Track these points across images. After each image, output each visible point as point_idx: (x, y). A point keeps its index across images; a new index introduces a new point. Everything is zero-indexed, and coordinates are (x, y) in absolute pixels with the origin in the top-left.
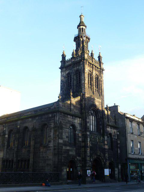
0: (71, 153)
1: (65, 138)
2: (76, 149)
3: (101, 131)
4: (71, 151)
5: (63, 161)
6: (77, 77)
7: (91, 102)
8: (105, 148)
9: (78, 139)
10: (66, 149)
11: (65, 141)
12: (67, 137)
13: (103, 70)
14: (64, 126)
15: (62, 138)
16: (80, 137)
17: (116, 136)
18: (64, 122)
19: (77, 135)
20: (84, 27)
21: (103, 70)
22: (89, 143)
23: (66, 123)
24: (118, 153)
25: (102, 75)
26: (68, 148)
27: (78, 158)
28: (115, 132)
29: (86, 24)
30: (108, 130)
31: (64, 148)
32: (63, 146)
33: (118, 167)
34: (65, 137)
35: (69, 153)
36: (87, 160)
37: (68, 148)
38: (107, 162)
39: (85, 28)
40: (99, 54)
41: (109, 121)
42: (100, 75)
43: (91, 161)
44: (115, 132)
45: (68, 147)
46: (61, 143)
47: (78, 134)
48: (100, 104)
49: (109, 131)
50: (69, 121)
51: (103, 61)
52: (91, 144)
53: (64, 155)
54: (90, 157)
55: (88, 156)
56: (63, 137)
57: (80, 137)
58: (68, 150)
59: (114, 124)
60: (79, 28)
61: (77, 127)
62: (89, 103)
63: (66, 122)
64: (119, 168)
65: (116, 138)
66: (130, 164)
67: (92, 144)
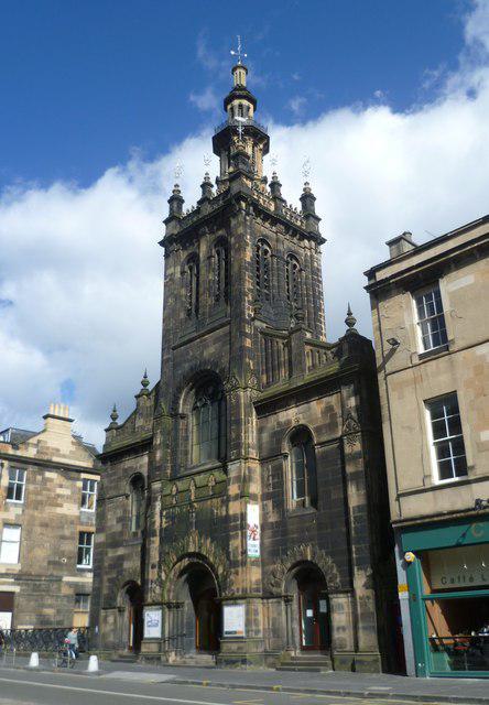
1: (112, 525)
8: (227, 515)
22: (157, 518)
26: (121, 551)
31: (111, 554)
32: (109, 550)
33: (351, 591)
34: (115, 523)
35: (122, 565)
37: (121, 551)
38: (237, 573)
43: (161, 584)
49: (289, 422)
50: (125, 470)
52: (164, 520)
53: (109, 576)
54: (160, 568)
55: (153, 567)
56: (109, 524)
58: (121, 558)
66: (410, 556)
67: (171, 517)
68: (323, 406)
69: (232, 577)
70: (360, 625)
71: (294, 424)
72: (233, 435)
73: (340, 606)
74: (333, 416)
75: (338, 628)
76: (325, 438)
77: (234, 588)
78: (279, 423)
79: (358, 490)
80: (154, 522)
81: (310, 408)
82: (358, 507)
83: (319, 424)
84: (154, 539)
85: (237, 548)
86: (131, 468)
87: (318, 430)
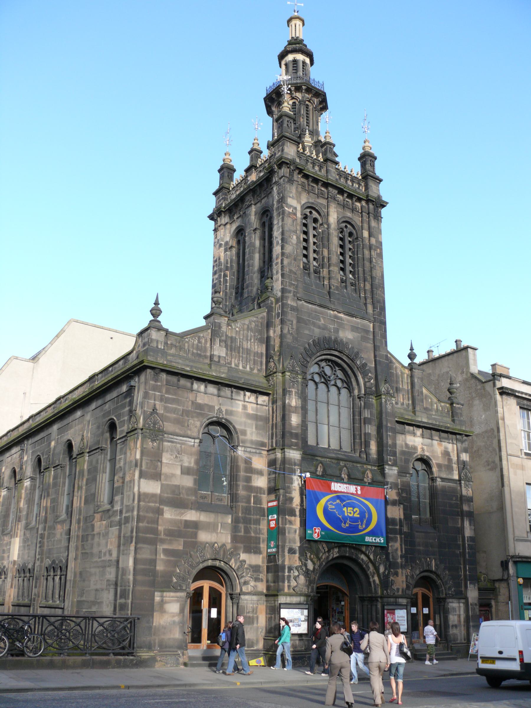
0: (204, 537)
1: (173, 475)
2: (236, 521)
3: (367, 445)
4: (211, 527)
5: (160, 567)
6: (264, 239)
7: (317, 331)
9: (248, 480)
10: (181, 520)
11: (178, 487)
12: (186, 471)
13: (381, 204)
14: (168, 426)
15: (156, 476)
16: (260, 473)
17: (455, 466)
18: (174, 411)
19: (242, 465)
20: (300, 57)
21: (381, 204)
23: (185, 413)
24: (464, 537)
25: (373, 224)
26: (191, 516)
27: (243, 556)
28: (446, 453)
29: (310, 46)
30: (410, 443)
32: (165, 508)
34: (178, 472)
35: (195, 535)
36: (283, 567)
37: (191, 516)
38: (396, 574)
39: (308, 61)
40: (364, 148)
41: (418, 408)
42: (366, 226)
44: (446, 453)
45: (193, 512)
46: (154, 495)
47: (248, 462)
48: (364, 339)
49: (415, 448)
50: (200, 407)
51: (379, 170)
53: (166, 546)
56: (165, 470)
57: (260, 473)
58: (195, 525)
59: (449, 420)
60: (283, 63)
61: (244, 433)
62: (307, 332)
63: (183, 410)
64: (466, 598)
65: (456, 477)
66: (521, 581)
68: (443, 448)
69: (392, 578)
70: (471, 624)
71: (419, 452)
72: (390, 442)
73: (454, 609)
74: (450, 460)
75: (453, 626)
76: (444, 476)
77: (395, 587)
78: (407, 445)
79: (470, 525)
80: (291, 499)
81: (432, 445)
82: (470, 537)
83: (440, 461)
84: (293, 518)
85: (397, 550)
86: (211, 408)
87: (439, 466)
